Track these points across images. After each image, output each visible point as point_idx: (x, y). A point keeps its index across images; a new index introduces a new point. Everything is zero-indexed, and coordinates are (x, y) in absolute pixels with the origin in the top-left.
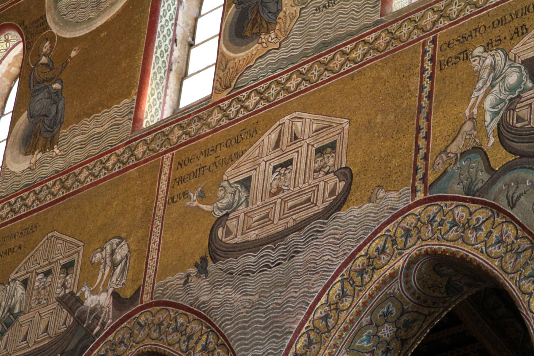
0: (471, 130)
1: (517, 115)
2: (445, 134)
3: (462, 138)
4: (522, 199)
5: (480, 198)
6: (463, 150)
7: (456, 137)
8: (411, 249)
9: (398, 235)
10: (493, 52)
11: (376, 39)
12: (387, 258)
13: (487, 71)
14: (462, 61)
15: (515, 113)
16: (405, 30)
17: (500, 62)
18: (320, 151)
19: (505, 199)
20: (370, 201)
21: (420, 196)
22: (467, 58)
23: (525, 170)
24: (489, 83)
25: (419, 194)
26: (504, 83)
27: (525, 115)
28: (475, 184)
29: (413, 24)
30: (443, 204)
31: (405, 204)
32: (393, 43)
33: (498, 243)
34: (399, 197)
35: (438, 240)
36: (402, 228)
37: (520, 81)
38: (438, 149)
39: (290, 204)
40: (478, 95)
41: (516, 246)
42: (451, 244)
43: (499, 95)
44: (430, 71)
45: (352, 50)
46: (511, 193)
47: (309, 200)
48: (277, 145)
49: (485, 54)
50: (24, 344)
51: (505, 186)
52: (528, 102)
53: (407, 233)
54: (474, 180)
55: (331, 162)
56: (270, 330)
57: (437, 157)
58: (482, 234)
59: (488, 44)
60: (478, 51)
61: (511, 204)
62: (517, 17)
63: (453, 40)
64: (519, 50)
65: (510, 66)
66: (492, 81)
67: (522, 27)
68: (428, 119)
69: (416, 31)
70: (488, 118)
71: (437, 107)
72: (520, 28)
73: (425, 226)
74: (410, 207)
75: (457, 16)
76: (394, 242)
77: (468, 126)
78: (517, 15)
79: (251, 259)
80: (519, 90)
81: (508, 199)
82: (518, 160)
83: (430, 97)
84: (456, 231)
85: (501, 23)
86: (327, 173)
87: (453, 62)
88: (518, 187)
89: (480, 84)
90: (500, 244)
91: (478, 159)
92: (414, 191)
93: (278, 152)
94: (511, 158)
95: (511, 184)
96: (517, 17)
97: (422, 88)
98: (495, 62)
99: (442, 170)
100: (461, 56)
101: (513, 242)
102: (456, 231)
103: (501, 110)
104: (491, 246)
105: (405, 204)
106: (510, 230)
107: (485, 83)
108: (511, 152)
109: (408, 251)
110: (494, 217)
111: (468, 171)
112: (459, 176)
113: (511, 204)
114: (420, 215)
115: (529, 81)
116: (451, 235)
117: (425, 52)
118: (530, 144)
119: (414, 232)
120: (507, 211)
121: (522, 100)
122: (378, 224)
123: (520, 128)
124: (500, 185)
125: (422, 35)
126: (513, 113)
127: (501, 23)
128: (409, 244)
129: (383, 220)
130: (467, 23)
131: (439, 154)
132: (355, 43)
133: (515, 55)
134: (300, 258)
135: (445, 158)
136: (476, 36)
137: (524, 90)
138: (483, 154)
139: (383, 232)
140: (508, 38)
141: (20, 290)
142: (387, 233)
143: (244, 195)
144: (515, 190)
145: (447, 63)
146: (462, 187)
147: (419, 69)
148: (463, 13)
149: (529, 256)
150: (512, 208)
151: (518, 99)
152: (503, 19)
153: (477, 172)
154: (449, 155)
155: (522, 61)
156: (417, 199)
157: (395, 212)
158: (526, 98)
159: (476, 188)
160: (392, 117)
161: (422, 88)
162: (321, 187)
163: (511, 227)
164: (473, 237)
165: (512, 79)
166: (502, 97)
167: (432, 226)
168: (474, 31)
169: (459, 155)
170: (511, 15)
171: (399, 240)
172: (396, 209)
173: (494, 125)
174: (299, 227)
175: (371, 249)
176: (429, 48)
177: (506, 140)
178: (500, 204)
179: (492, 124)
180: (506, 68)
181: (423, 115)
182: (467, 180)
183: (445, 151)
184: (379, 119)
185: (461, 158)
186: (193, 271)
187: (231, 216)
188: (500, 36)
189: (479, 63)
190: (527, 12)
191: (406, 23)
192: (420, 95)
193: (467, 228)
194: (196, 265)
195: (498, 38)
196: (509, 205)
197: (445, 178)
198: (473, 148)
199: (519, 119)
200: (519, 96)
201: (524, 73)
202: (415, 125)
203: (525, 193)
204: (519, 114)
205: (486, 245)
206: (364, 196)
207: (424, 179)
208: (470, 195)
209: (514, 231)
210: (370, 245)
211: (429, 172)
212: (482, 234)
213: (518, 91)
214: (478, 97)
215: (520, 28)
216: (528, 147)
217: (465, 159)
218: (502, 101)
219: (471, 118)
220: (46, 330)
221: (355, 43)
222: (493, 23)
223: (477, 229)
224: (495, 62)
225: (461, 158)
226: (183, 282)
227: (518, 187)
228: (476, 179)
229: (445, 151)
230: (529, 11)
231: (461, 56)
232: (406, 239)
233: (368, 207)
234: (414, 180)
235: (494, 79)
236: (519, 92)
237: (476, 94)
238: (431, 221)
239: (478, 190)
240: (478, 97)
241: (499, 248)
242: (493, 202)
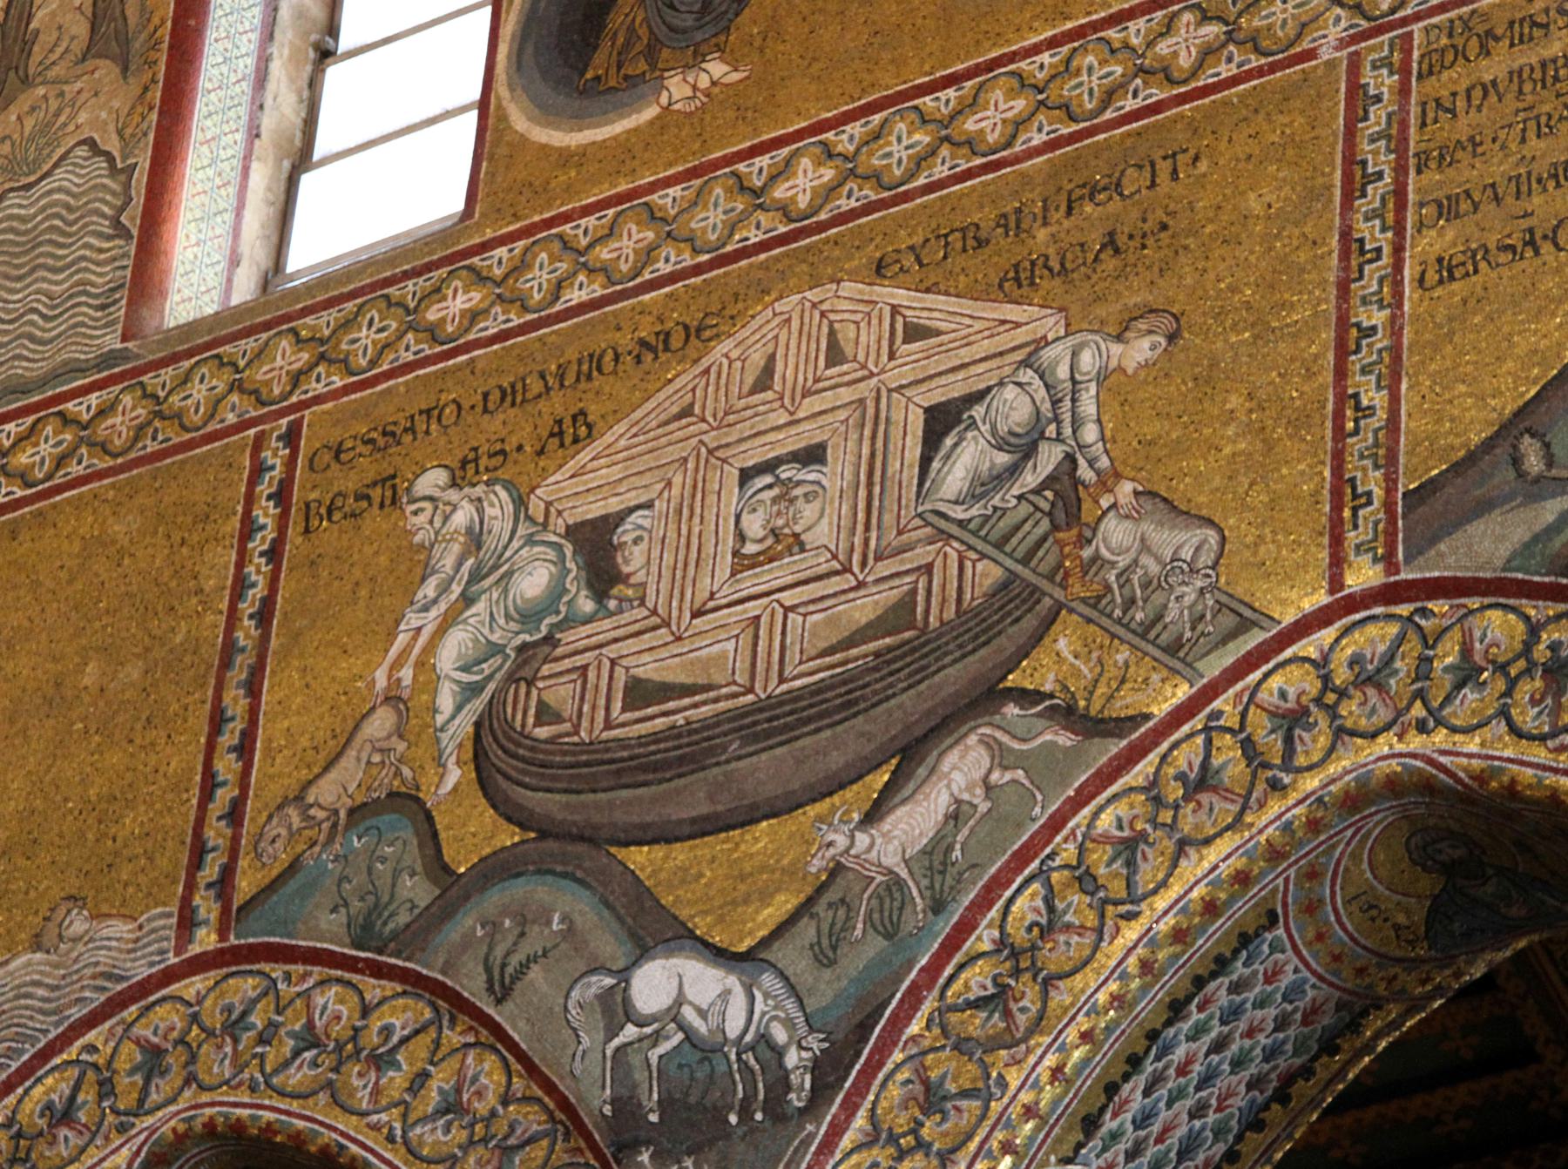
0: (389, 737)
1: (540, 702)
2: (304, 742)
3: (358, 759)
4: (535, 973)
5: (400, 963)
6: (360, 799)
7: (339, 755)
8: (160, 1114)
9: (122, 1064)
10: (479, 490)
11: (102, 413)
12: (76, 1141)
13: (456, 548)
14: (375, 510)
15: (535, 692)
16: (198, 392)
17: (497, 525)
19: (481, 969)
20: (37, 944)
21: (205, 940)
22: (394, 502)
23: (549, 879)
24: (456, 590)
25: (201, 933)
26: (506, 591)
27: (565, 701)
28: (386, 914)
29: (227, 375)
30: (277, 971)
31: (152, 964)
32: (156, 430)
33: (447, 1111)
34: (137, 940)
35: (253, 1089)
36: (137, 1042)
37: (557, 591)
38: (275, 792)
40: (420, 623)
41: (501, 1127)
42: (295, 1106)
43: (486, 631)
44: (270, 534)
45: (20, 439)
46: (499, 952)
49: (453, 495)
51: (483, 927)
52: (579, 661)
53: (154, 1061)
54: (386, 898)
57: (270, 817)
58: (395, 1080)
59: (464, 463)
60: (432, 480)
61: (497, 987)
62: (562, 385)
63: (355, 438)
64: (562, 489)
65: (530, 541)
66: (468, 582)
67: (574, 418)
68: (253, 688)
69: (235, 398)
70: (446, 702)
71: (285, 653)
72: (568, 421)
73: (212, 1040)
74: (170, 976)
75: (373, 363)
76: (106, 1088)
77: (380, 723)
78: (562, 378)
80: (554, 619)
81: (488, 970)
82: (532, 845)
83: (264, 615)
84: (314, 1064)
85: (509, 399)
87: (347, 509)
88: (522, 934)
89: (429, 589)
90: (450, 1117)
91: (402, 834)
92: (187, 922)
94: (509, 836)
95: (502, 923)
96: (562, 385)
97: (240, 585)
98: (482, 523)
99: (285, 859)
100: (376, 494)
101: (493, 1114)
102: (314, 1064)
103: (490, 677)
104: (424, 1120)
105: (152, 964)
106: (488, 1072)
107: (444, 589)
108: (509, 820)
109: (149, 1121)
110: (441, 1028)
111: (370, 870)
112: (339, 885)
113: (497, 987)
114: (199, 1003)
115: (584, 593)
116: (296, 1077)
117: (258, 470)
118: (573, 798)
119: (174, 1060)
120: (481, 1011)
121: (559, 651)
122: (57, 1024)
123: (546, 741)
124: (467, 922)
125: (254, 414)
126: (528, 694)
127: (509, 399)
128: (154, 1097)
129: (76, 1013)
130: (402, 389)
131: (280, 807)
132: (30, 419)
133: (548, 504)
135: (296, 821)
136: (427, 432)
137: (566, 619)
138: (421, 816)
139: (71, 1053)
140: (528, 448)
142: (84, 1057)
144: (515, 944)
145: (330, 512)
146: (344, 920)
147: (236, 522)
148: (392, 357)
149: (539, 1162)
150: (499, 1002)
151: (546, 649)
152: (519, 386)
153: (396, 874)
154: (312, 812)
155: (568, 527)
156: (195, 949)
157: (119, 988)
158: (571, 647)
159: (391, 926)
160: (134, 672)
161: (240, 585)
163: (490, 1061)
164: (365, 1086)
165: (533, 582)
166: (494, 638)
167: (236, 1041)
168: (424, 417)
169: (343, 814)
170: (543, 377)
171: (123, 1082)
172: (121, 979)
173: (464, 725)
175: (28, 1106)
176: (275, 456)
177: (499, 778)
178: (462, 986)
179: (457, 722)
180: (515, 544)
181: (238, 673)
182: (362, 899)
183: (299, 798)
184: (91, 675)
185: (347, 828)
188: (503, 441)
189: (431, 522)
190: (595, 373)
191: (204, 370)
192: (233, 608)
193: (349, 1057)
195: (498, 447)
196: (490, 989)
197: (292, 885)
198: (391, 795)
199: (545, 714)
200: (549, 640)
201: (571, 565)
202: (208, 706)
203: (544, 955)
204: (546, 696)
205: (404, 1116)
206: (20, 926)
207: (224, 884)
208: (369, 950)
209: (499, 1077)
210: (26, 1092)
211: (243, 863)
212: (395, 1080)
213: (547, 621)
214: (419, 629)
215: (568, 421)
216: (567, 806)
217: (361, 828)
218: (496, 649)
219: (392, 698)
221: (30, 419)
222: (486, 395)
223: (380, 1062)
224: (482, 523)
225: (347, 828)
227: (522, 934)
228: (392, 896)
229: (299, 798)
230: (599, 370)
231: (376, 494)
232: (147, 1081)
233: (29, 964)
234: (190, 887)
235: (476, 576)
236: (552, 625)
237: (412, 620)
238: (234, 1026)
239: (395, 935)
240: (419, 629)
241: (447, 1130)
242: (440, 977)
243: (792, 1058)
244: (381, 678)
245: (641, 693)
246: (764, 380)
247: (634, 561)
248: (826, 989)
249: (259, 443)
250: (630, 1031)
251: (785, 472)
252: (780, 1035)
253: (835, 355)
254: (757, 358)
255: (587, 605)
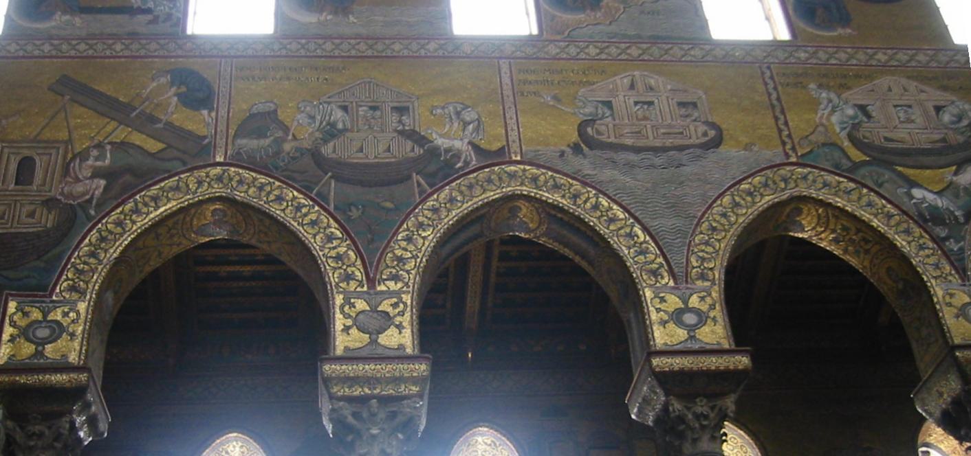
18: (682, 104)
20: (745, 149)
21: (793, 159)
39: (662, 131)
47: (682, 133)
48: (632, 87)
50: (360, 155)
55: (696, 114)
56: (674, 210)
68: (783, 112)
70: (838, 130)
76: (775, 183)
77: (821, 129)
79: (633, 157)
83: (778, 99)
86: (695, 120)
92: (787, 155)
93: (634, 92)
109: (788, 191)
117: (763, 73)
129: (763, 166)
134: (687, 170)
139: (763, 173)
141: (338, 114)
143: (608, 113)
162: (692, 128)
165: (850, 112)
172: (773, 162)
174: (681, 148)
181: (778, 110)
186: (568, 150)
187: (598, 122)
194: (569, 146)
199: (864, 137)
220: (388, 150)
226: (558, 154)
238: (805, 178)
243: (957, 213)
244: (817, 120)
245: (886, 139)
246: (890, 90)
247: (874, 114)
248: (960, 203)
249: (760, 67)
250: (914, 201)
251: (905, 108)
252: (952, 209)
253: (906, 90)
254: (886, 87)
255: (866, 120)
